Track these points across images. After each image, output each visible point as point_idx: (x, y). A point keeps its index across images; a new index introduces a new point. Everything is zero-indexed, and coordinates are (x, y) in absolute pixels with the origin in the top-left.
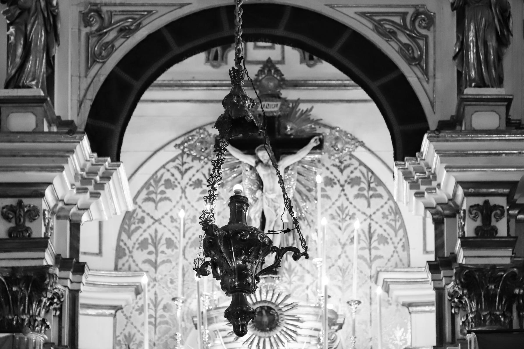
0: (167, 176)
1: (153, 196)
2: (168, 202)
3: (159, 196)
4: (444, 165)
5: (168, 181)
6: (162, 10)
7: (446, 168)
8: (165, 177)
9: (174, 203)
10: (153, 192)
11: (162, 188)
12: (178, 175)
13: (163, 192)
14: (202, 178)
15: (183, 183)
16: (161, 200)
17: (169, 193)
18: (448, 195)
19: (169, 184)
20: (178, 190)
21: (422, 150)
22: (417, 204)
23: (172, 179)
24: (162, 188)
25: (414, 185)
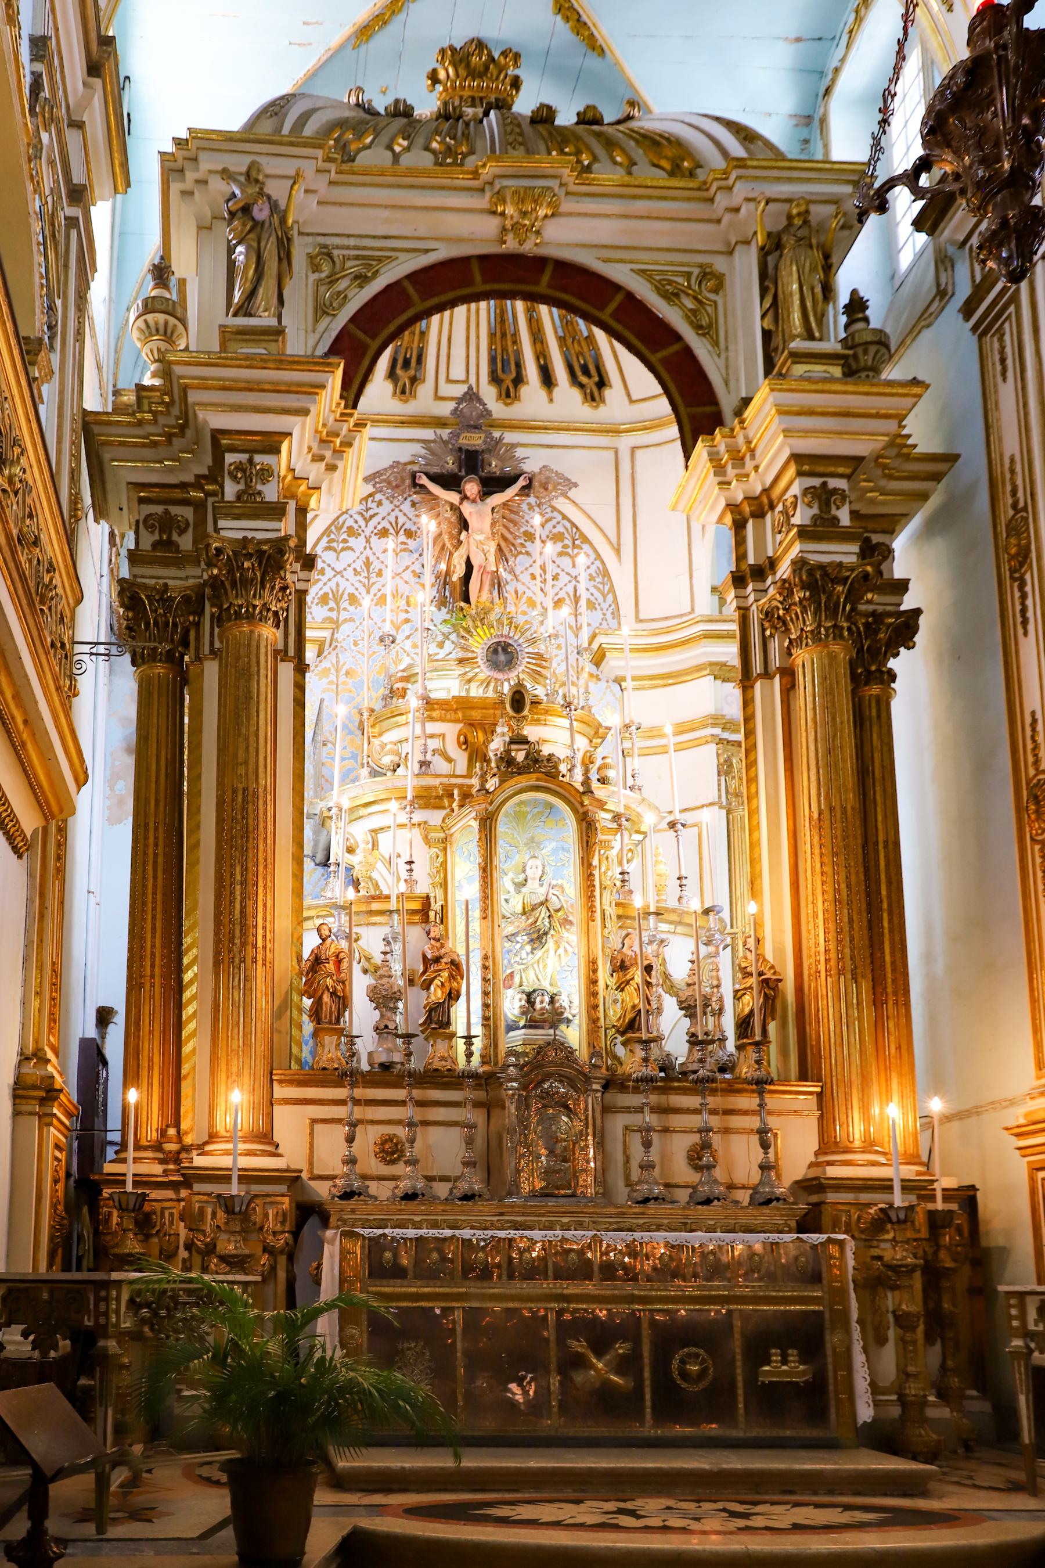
0: (350, 522)
1: (335, 545)
2: (350, 552)
3: (341, 545)
4: (783, 426)
5: (350, 528)
6: (403, 256)
7: (784, 431)
8: (347, 524)
9: (358, 553)
10: (333, 541)
11: (345, 536)
12: (362, 523)
13: (345, 541)
14: (388, 526)
15: (368, 532)
16: (343, 549)
17: (352, 542)
18: (763, 483)
19: (351, 532)
20: (362, 539)
21: (746, 415)
22: (716, 499)
23: (356, 526)
24: (345, 536)
25: (719, 469)
